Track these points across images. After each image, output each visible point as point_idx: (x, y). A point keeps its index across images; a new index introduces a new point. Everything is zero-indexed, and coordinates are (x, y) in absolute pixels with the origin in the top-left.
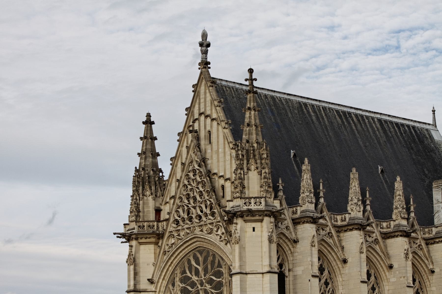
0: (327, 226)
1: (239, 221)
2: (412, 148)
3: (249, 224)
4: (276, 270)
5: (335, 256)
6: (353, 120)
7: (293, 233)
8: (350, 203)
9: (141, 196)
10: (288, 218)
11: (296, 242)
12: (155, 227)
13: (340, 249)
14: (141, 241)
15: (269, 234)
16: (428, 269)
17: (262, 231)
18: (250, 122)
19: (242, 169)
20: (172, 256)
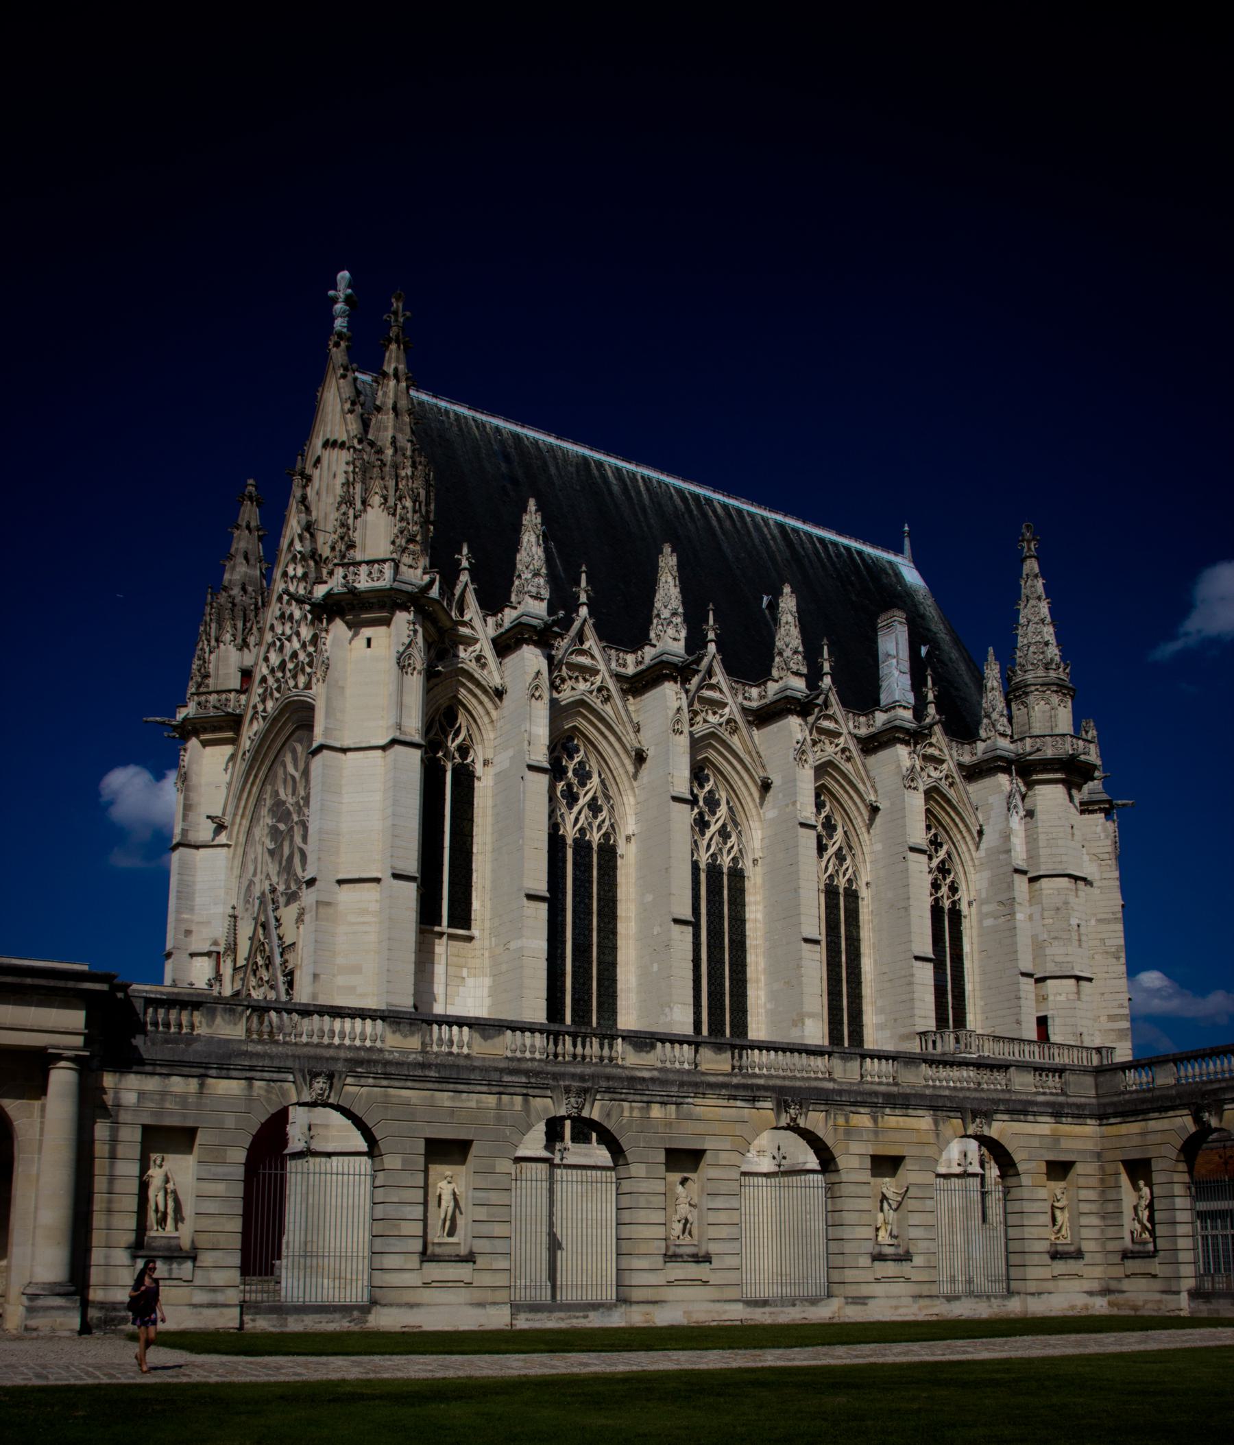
0: (597, 672)
1: (339, 628)
4: (417, 738)
5: (617, 745)
6: (714, 511)
7: (496, 674)
8: (655, 621)
10: (481, 635)
11: (499, 693)
15: (401, 649)
16: (866, 806)
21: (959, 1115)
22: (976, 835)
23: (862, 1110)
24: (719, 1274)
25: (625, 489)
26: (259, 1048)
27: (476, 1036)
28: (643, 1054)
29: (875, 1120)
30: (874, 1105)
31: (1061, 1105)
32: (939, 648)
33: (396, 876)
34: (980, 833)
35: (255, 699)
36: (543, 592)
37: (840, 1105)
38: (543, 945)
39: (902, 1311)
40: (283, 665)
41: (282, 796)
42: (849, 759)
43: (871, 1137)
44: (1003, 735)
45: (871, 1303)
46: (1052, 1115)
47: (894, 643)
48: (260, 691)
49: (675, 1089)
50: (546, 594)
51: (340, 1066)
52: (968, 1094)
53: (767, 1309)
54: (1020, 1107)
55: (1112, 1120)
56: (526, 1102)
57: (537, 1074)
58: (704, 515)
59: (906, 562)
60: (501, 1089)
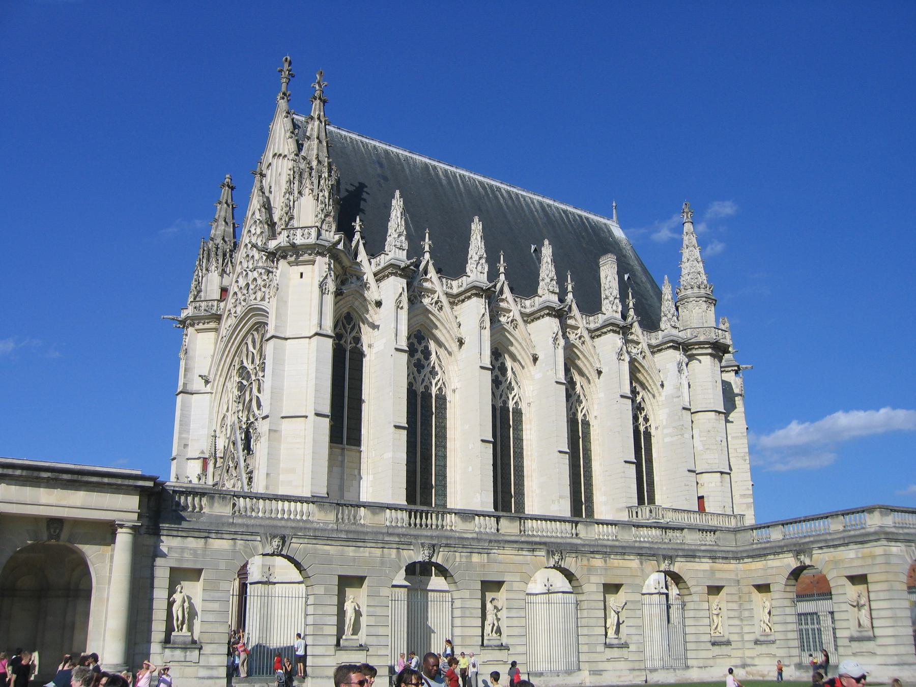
2: (583, 237)
4: (330, 332)
6: (502, 195)
9: (204, 271)
12: (215, 308)
13: (455, 325)
14: (197, 327)
17: (312, 278)
18: (311, 135)
19: (291, 193)
20: (229, 341)
22: (659, 387)
23: (597, 556)
25: (450, 182)
26: (240, 521)
29: (605, 561)
32: (635, 275)
33: (317, 415)
34: (662, 385)
35: (230, 305)
37: (583, 553)
39: (622, 679)
40: (248, 285)
41: (245, 364)
44: (675, 327)
45: (604, 673)
46: (710, 558)
47: (608, 273)
48: (233, 301)
50: (406, 245)
52: (660, 546)
53: (542, 678)
54: (690, 553)
55: (746, 560)
56: (398, 553)
58: (496, 197)
59: (615, 224)
60: (384, 545)
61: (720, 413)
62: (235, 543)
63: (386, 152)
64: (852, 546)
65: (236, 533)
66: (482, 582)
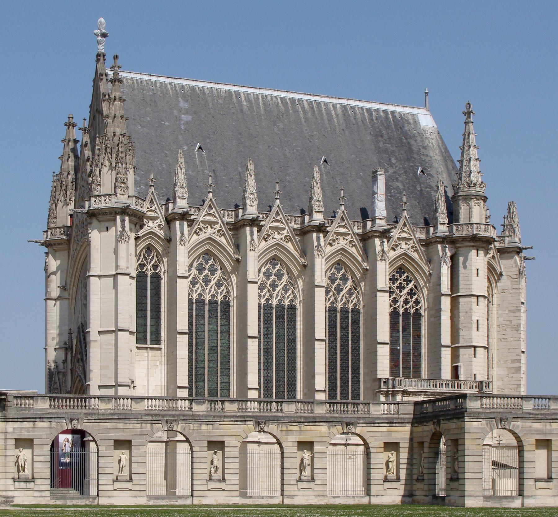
0: (218, 223)
2: (382, 136)
3: (103, 223)
6: (303, 108)
21: (340, 424)
23: (294, 424)
24: (229, 486)
25: (251, 108)
27: (133, 402)
28: (200, 406)
29: (300, 428)
30: (300, 422)
31: (393, 418)
36: (185, 195)
38: (187, 353)
42: (353, 246)
43: (298, 434)
46: (388, 423)
49: (211, 419)
50: (186, 196)
51: (82, 416)
53: (251, 500)
56: (152, 426)
57: (156, 415)
59: (425, 112)
60: (142, 421)
61: (478, 296)
62: (51, 424)
63: (193, 89)
64: (455, 420)
65: (51, 418)
66: (209, 442)
